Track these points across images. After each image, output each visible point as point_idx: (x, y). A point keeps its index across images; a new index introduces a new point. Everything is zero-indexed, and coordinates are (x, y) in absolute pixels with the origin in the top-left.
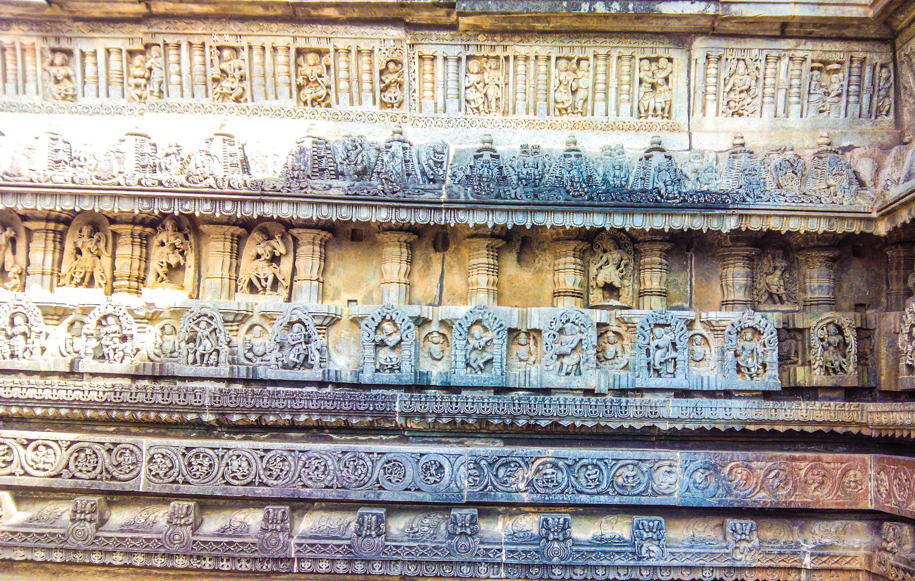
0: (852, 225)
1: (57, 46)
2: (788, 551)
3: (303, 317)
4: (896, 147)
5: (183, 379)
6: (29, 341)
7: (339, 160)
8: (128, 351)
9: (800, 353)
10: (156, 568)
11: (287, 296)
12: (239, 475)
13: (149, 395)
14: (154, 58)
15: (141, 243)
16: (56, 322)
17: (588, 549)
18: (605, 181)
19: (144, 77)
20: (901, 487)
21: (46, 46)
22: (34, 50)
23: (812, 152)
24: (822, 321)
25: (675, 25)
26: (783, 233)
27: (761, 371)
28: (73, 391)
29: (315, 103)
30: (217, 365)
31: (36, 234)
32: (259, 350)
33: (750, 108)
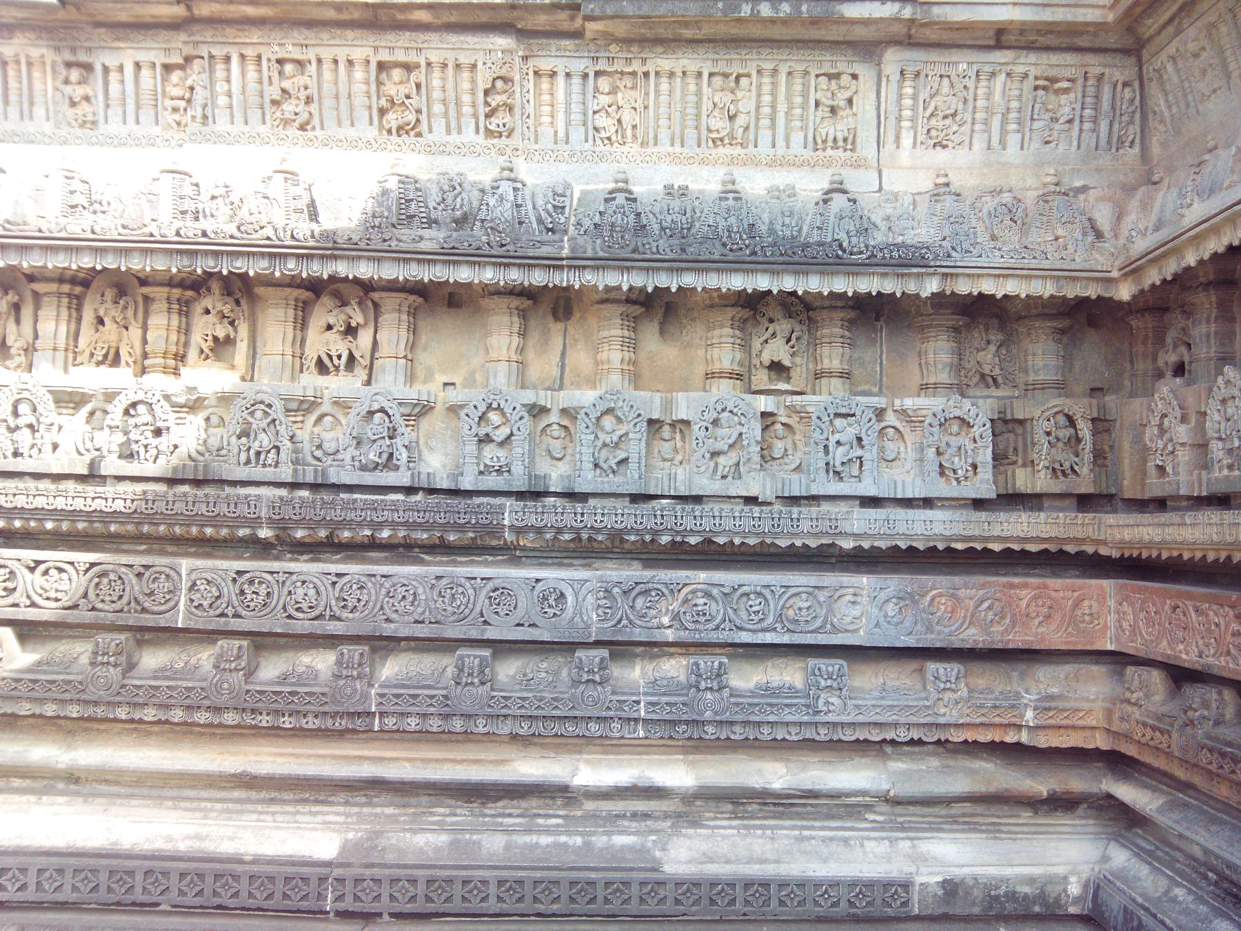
0: (1086, 287)
1: (71, 58)
2: (1005, 704)
3: (386, 405)
4: (1143, 188)
5: (234, 483)
6: (37, 435)
7: (431, 205)
8: (163, 448)
9: (1020, 451)
10: (199, 725)
11: (366, 378)
12: (304, 606)
13: (190, 504)
14: (196, 75)
15: (180, 310)
16: (71, 411)
17: (750, 700)
18: (772, 231)
19: (182, 98)
20: (1150, 622)
21: (58, 59)
22: (44, 63)
23: (1035, 193)
24: (1048, 409)
25: (860, 33)
26: (999, 296)
27: (970, 474)
28: (93, 499)
29: (402, 132)
30: (276, 466)
31: (46, 299)
32: (330, 446)
33: (957, 138)
